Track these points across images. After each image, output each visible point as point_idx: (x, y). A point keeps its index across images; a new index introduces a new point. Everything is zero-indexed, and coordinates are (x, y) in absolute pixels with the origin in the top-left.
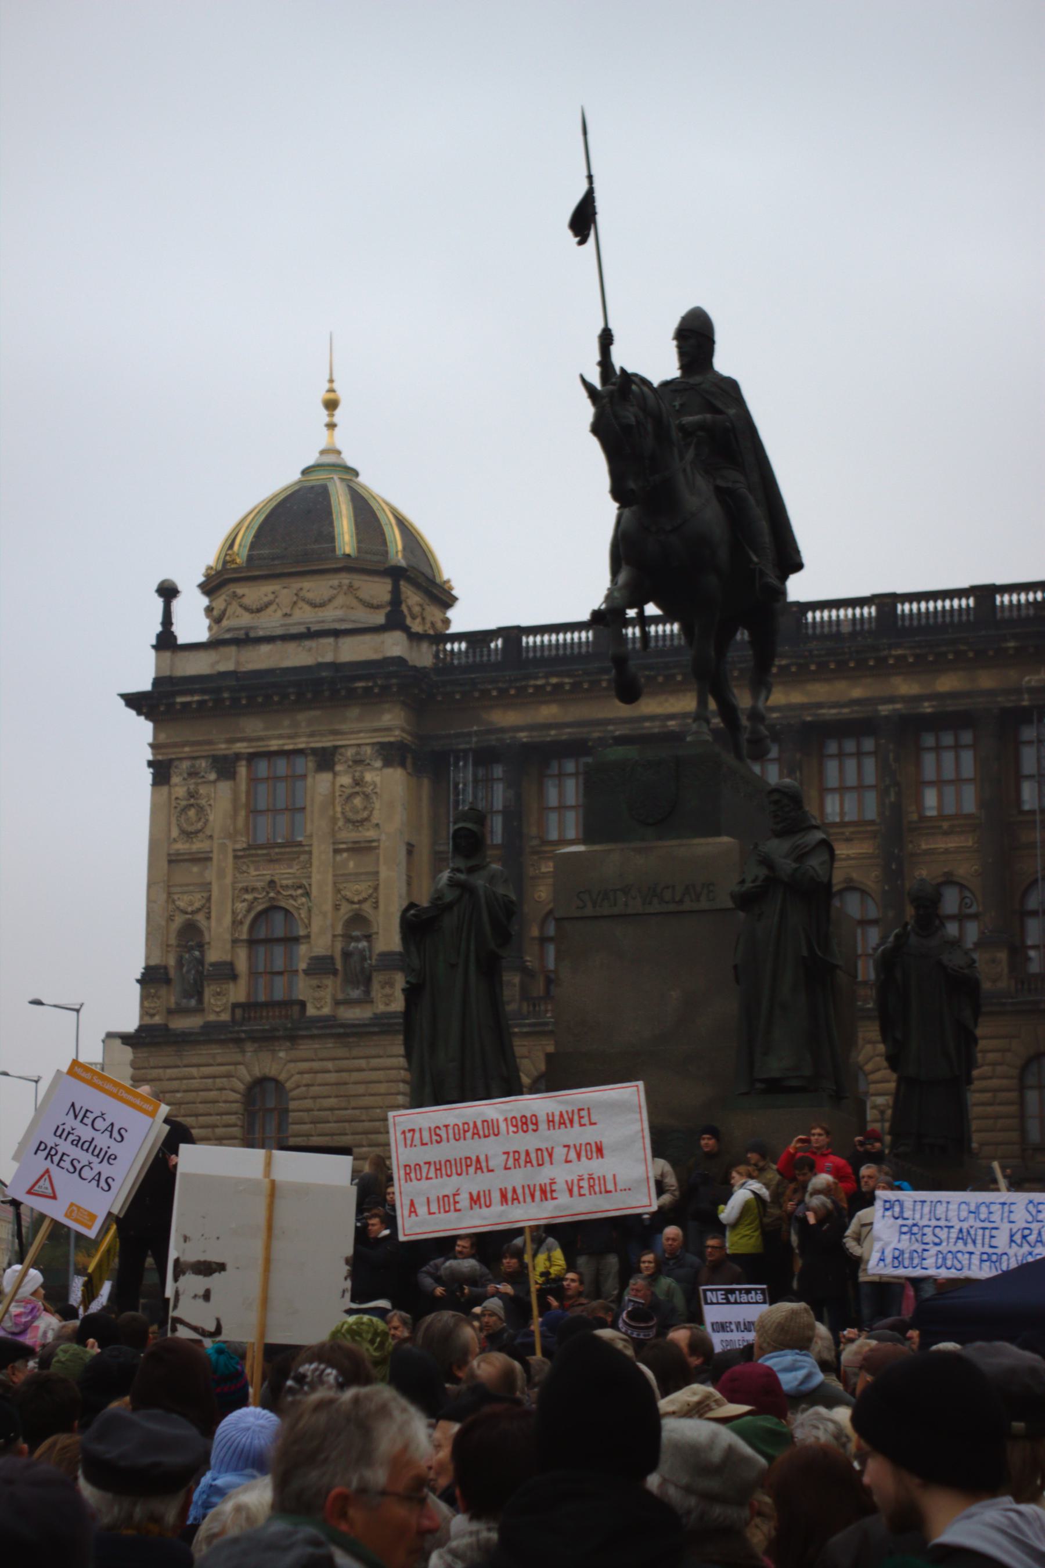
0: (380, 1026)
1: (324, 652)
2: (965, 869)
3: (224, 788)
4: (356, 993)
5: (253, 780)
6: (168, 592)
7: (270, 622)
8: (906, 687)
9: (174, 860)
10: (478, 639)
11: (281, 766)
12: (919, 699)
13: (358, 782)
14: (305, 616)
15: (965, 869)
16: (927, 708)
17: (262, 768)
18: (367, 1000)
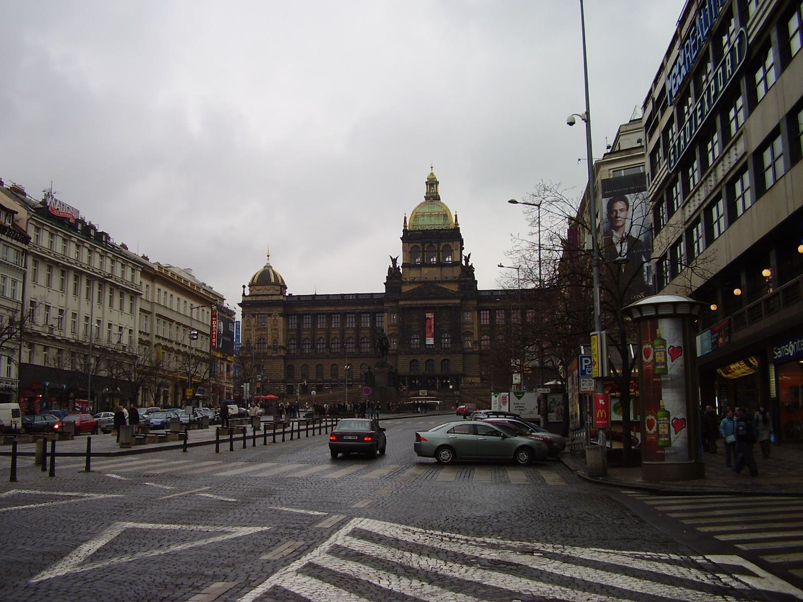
0: (280, 357)
1: (270, 298)
2: (368, 336)
3: (253, 319)
4: (275, 352)
5: (258, 318)
6: (244, 287)
7: (261, 293)
8: (360, 308)
9: (245, 330)
10: (290, 295)
11: (262, 315)
12: (362, 310)
13: (275, 319)
14: (266, 292)
15: (368, 336)
16: (363, 311)
17: (259, 315)
18: (276, 353)
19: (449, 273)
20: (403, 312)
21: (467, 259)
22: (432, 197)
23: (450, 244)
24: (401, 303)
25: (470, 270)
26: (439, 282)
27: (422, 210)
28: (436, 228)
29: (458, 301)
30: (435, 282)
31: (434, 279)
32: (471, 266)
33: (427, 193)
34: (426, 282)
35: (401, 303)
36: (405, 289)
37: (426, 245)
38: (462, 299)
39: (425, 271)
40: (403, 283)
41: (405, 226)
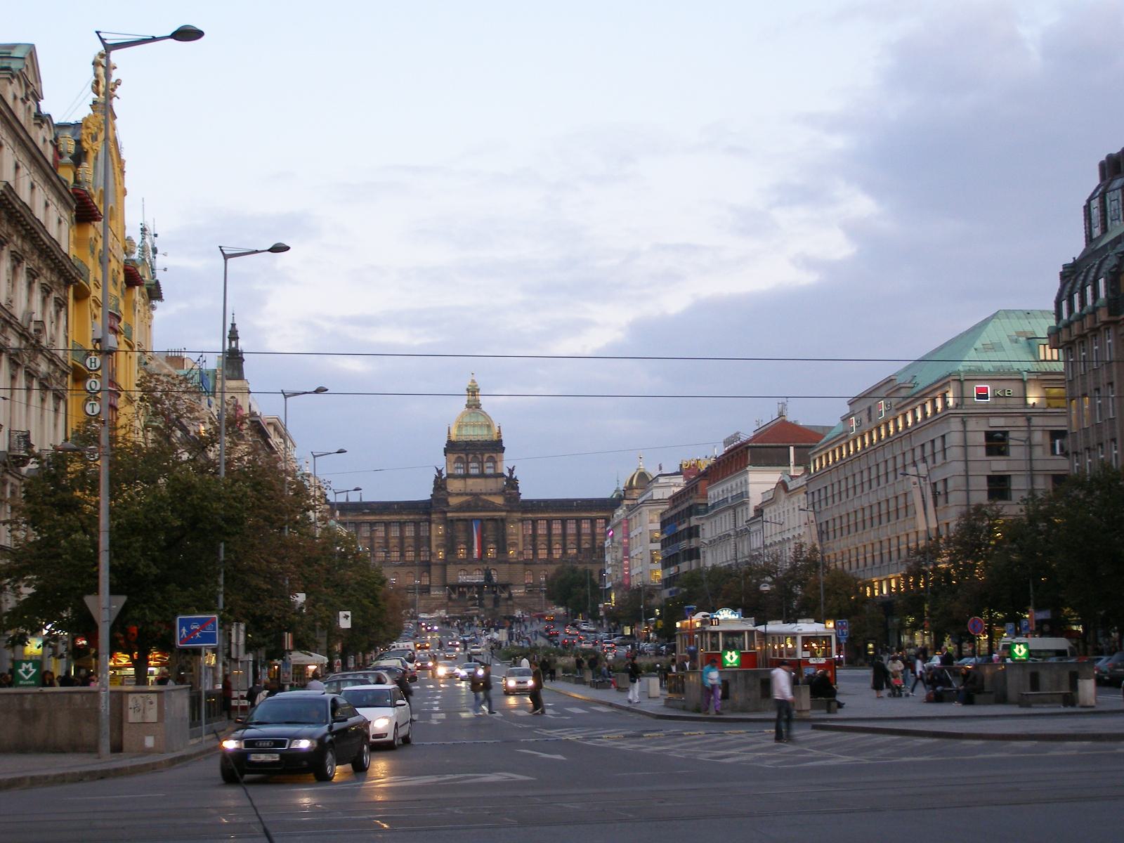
8: (405, 517)
19: (492, 484)
20: (449, 523)
21: (511, 471)
22: (474, 406)
23: (494, 455)
24: (449, 515)
25: (512, 483)
26: (485, 494)
27: (466, 420)
28: (480, 438)
29: (504, 514)
30: (481, 494)
31: (478, 491)
32: (515, 479)
33: (468, 401)
34: (471, 494)
35: (449, 515)
36: (453, 501)
37: (471, 456)
38: (508, 511)
39: (470, 481)
40: (450, 494)
41: (449, 437)
